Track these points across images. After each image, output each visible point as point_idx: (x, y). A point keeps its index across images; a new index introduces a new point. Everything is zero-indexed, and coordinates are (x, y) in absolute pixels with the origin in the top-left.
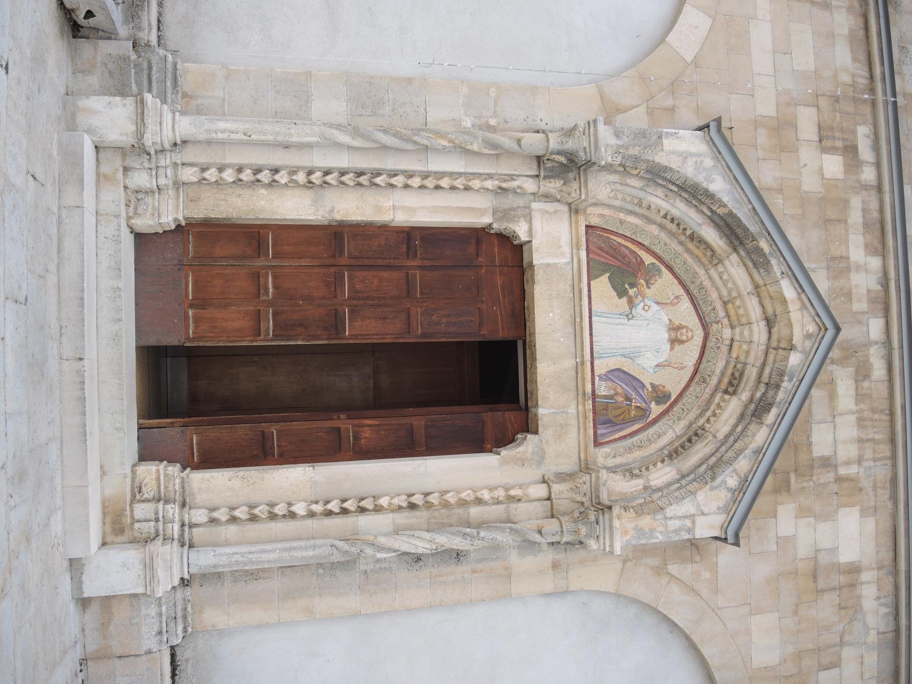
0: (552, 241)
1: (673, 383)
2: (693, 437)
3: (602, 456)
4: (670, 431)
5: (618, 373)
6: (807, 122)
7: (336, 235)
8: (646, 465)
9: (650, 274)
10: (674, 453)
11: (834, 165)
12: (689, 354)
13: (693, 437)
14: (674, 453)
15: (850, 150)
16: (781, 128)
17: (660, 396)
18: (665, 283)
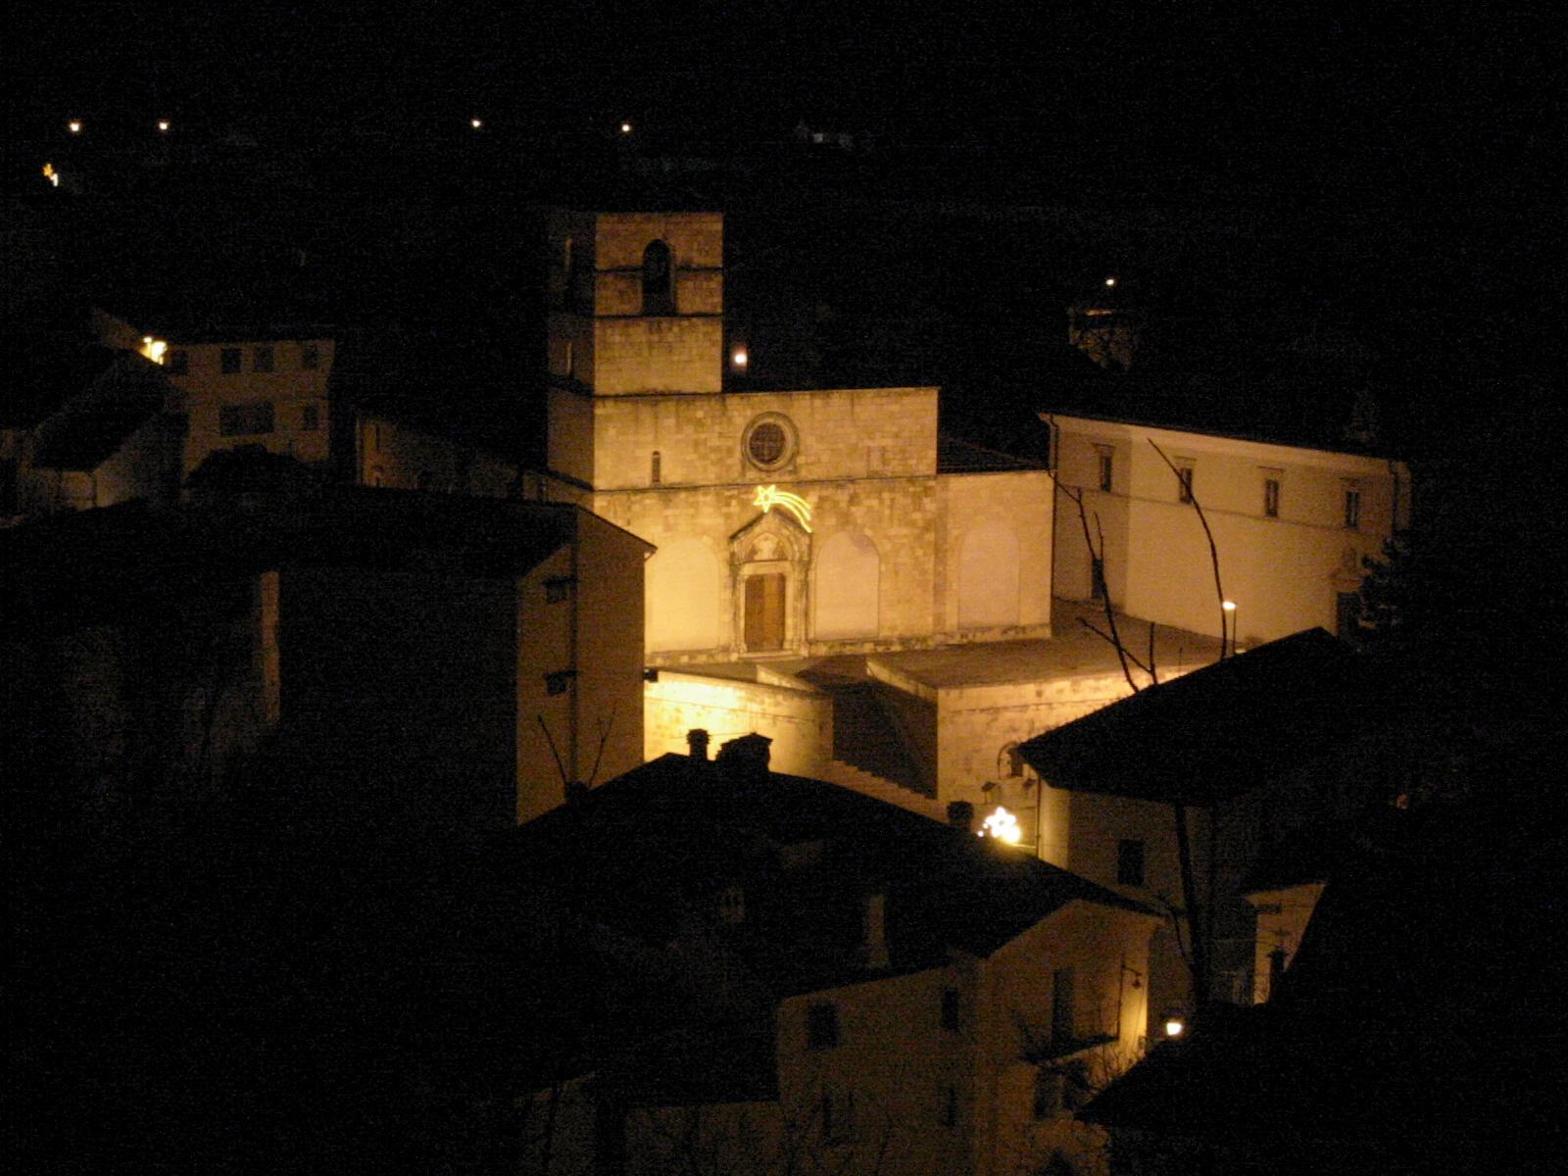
0: (747, 571)
1: (776, 540)
2: (788, 539)
3: (790, 558)
4: (788, 545)
5: (774, 553)
6: (725, 510)
7: (747, 614)
8: (793, 550)
9: (753, 546)
10: (791, 544)
11: (734, 502)
12: (771, 536)
13: (788, 539)
14: (791, 544)
15: (731, 497)
16: (728, 516)
17: (778, 543)
18: (756, 541)
